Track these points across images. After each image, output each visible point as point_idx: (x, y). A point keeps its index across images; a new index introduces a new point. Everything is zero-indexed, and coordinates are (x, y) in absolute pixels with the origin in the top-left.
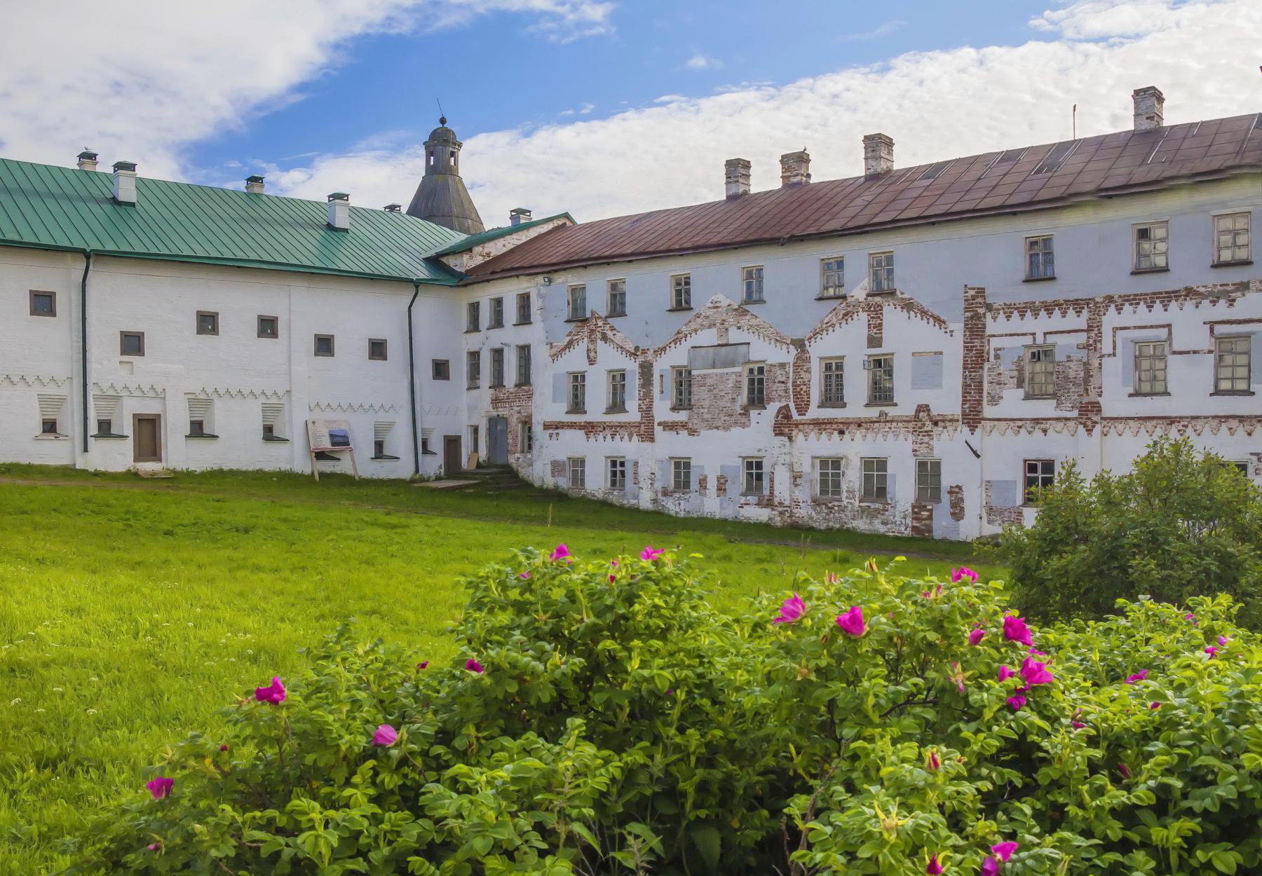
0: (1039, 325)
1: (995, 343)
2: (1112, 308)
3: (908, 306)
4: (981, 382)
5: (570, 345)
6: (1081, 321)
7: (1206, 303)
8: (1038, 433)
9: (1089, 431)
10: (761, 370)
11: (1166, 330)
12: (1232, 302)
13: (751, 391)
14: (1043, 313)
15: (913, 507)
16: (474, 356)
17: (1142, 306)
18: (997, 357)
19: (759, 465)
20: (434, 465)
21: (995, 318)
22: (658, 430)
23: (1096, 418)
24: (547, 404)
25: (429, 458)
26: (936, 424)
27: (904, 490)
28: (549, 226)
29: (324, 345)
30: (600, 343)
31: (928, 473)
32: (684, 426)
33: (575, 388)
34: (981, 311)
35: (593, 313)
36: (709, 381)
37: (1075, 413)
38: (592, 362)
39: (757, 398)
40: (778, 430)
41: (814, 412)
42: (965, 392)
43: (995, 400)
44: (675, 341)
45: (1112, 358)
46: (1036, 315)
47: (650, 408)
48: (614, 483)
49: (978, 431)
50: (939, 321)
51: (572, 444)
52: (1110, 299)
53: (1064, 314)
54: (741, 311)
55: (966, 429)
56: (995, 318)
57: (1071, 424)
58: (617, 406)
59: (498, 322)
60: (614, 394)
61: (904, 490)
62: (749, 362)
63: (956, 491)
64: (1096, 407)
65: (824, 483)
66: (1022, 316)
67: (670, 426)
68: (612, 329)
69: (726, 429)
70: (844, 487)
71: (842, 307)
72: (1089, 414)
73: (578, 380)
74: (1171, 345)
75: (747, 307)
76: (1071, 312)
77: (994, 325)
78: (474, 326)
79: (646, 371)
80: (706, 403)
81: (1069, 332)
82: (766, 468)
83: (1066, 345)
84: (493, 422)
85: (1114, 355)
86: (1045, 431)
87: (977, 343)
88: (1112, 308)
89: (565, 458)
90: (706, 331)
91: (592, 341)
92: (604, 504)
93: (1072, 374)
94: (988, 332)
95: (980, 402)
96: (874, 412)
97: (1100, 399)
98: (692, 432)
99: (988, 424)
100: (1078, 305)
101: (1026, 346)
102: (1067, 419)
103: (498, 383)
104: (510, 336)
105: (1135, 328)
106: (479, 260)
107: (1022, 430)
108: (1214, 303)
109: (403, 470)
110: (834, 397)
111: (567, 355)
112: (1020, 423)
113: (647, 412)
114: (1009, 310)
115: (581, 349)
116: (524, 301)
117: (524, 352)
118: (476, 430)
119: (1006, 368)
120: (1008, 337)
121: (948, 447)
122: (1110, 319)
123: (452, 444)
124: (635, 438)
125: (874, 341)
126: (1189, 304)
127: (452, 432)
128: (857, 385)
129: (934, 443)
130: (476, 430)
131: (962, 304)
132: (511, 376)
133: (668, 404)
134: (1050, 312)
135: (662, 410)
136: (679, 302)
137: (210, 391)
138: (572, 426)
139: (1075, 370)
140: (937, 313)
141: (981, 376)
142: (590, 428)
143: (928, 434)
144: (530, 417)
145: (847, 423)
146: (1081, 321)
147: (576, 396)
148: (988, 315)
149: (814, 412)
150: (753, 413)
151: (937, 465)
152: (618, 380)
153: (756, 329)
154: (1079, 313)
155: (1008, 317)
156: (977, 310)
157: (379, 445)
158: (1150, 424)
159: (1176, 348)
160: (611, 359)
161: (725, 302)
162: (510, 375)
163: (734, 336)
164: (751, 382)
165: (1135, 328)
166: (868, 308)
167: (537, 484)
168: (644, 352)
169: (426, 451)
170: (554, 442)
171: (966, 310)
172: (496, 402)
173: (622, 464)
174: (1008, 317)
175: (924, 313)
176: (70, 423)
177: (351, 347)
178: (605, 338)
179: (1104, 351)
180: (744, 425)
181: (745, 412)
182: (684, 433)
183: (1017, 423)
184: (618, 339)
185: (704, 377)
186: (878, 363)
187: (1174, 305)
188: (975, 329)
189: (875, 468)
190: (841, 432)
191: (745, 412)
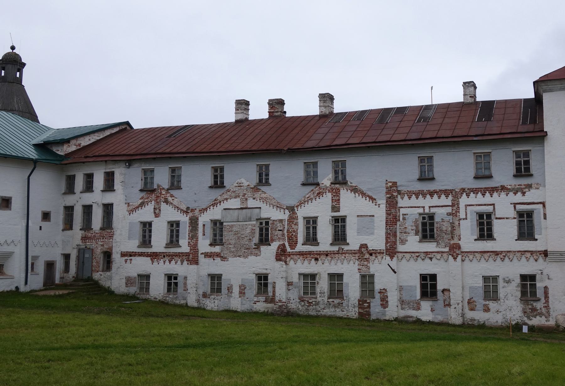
0: (427, 203)
1: (402, 211)
2: (464, 195)
3: (355, 190)
4: (396, 232)
5: (142, 205)
6: (449, 201)
7: (511, 194)
9: (455, 259)
11: (492, 206)
12: (524, 194)
13: (261, 235)
14: (428, 196)
15: (359, 301)
16: (69, 210)
17: (480, 195)
18: (404, 219)
19: (266, 277)
20: (37, 281)
21: (402, 198)
22: (201, 258)
26: (371, 255)
28: (116, 130)
30: (163, 206)
31: (367, 281)
32: (218, 255)
34: (395, 194)
35: (159, 186)
37: (447, 249)
38: (157, 215)
39: (264, 240)
41: (300, 247)
42: (387, 238)
43: (403, 242)
44: (213, 205)
45: (465, 221)
46: (424, 197)
47: (196, 245)
48: (169, 290)
49: (395, 259)
50: (372, 199)
51: (141, 265)
52: (463, 190)
53: (439, 197)
54: (256, 189)
55: (388, 258)
56: (402, 198)
57: (445, 255)
58: (173, 240)
60: (172, 236)
62: (260, 219)
63: (383, 292)
64: (459, 247)
65: (305, 287)
66: (417, 198)
67: (208, 255)
68: (172, 196)
69: (246, 257)
70: (318, 290)
71: (317, 190)
72: (455, 250)
73: (147, 227)
74: (495, 215)
75: (259, 187)
77: (403, 202)
78: (70, 190)
79: (194, 222)
80: (233, 242)
81: (442, 206)
82: (270, 280)
83: (441, 214)
84: (81, 252)
85: (466, 219)
86: (431, 259)
87: (393, 211)
88: (464, 195)
89: (136, 275)
90: (233, 200)
91: (158, 203)
92: (163, 303)
93: (444, 229)
94: (399, 205)
95: (395, 243)
96: (336, 248)
97: (460, 242)
98: (224, 259)
99: (400, 255)
100: (447, 193)
101: (420, 214)
102: (442, 252)
105: (476, 205)
107: (419, 258)
108: (515, 194)
110: (312, 239)
111: (140, 211)
112: (417, 254)
113: (194, 247)
115: (150, 207)
117: (108, 209)
118: (67, 257)
119: (409, 224)
121: (380, 269)
122: (464, 200)
123: (50, 266)
124: (185, 262)
125: (335, 208)
126: (503, 194)
127: (49, 259)
128: (325, 233)
129: (370, 265)
130: (67, 257)
133: (208, 242)
135: (204, 245)
136: (216, 183)
138: (141, 254)
139: (446, 226)
140: (370, 194)
141: (396, 228)
142: (154, 256)
144: (111, 249)
145: (320, 254)
146: (449, 201)
148: (399, 197)
149: (300, 247)
150: (263, 248)
151: (372, 276)
152: (174, 226)
153: (265, 200)
154: (447, 197)
155: (410, 198)
156: (393, 194)
158: (486, 255)
160: (169, 213)
161: (246, 183)
163: (251, 203)
164: (261, 230)
165: (476, 205)
166: (331, 190)
167: (117, 291)
168: (193, 210)
171: (387, 193)
172: (84, 239)
173: (176, 278)
174: (410, 198)
175: (363, 194)
178: (166, 202)
179: (461, 217)
180: (256, 255)
181: (257, 246)
182: (219, 259)
183: (416, 255)
184: (175, 202)
185: (232, 226)
187: (495, 194)
188: (392, 204)
189: (336, 278)
190: (316, 259)
191: (257, 246)
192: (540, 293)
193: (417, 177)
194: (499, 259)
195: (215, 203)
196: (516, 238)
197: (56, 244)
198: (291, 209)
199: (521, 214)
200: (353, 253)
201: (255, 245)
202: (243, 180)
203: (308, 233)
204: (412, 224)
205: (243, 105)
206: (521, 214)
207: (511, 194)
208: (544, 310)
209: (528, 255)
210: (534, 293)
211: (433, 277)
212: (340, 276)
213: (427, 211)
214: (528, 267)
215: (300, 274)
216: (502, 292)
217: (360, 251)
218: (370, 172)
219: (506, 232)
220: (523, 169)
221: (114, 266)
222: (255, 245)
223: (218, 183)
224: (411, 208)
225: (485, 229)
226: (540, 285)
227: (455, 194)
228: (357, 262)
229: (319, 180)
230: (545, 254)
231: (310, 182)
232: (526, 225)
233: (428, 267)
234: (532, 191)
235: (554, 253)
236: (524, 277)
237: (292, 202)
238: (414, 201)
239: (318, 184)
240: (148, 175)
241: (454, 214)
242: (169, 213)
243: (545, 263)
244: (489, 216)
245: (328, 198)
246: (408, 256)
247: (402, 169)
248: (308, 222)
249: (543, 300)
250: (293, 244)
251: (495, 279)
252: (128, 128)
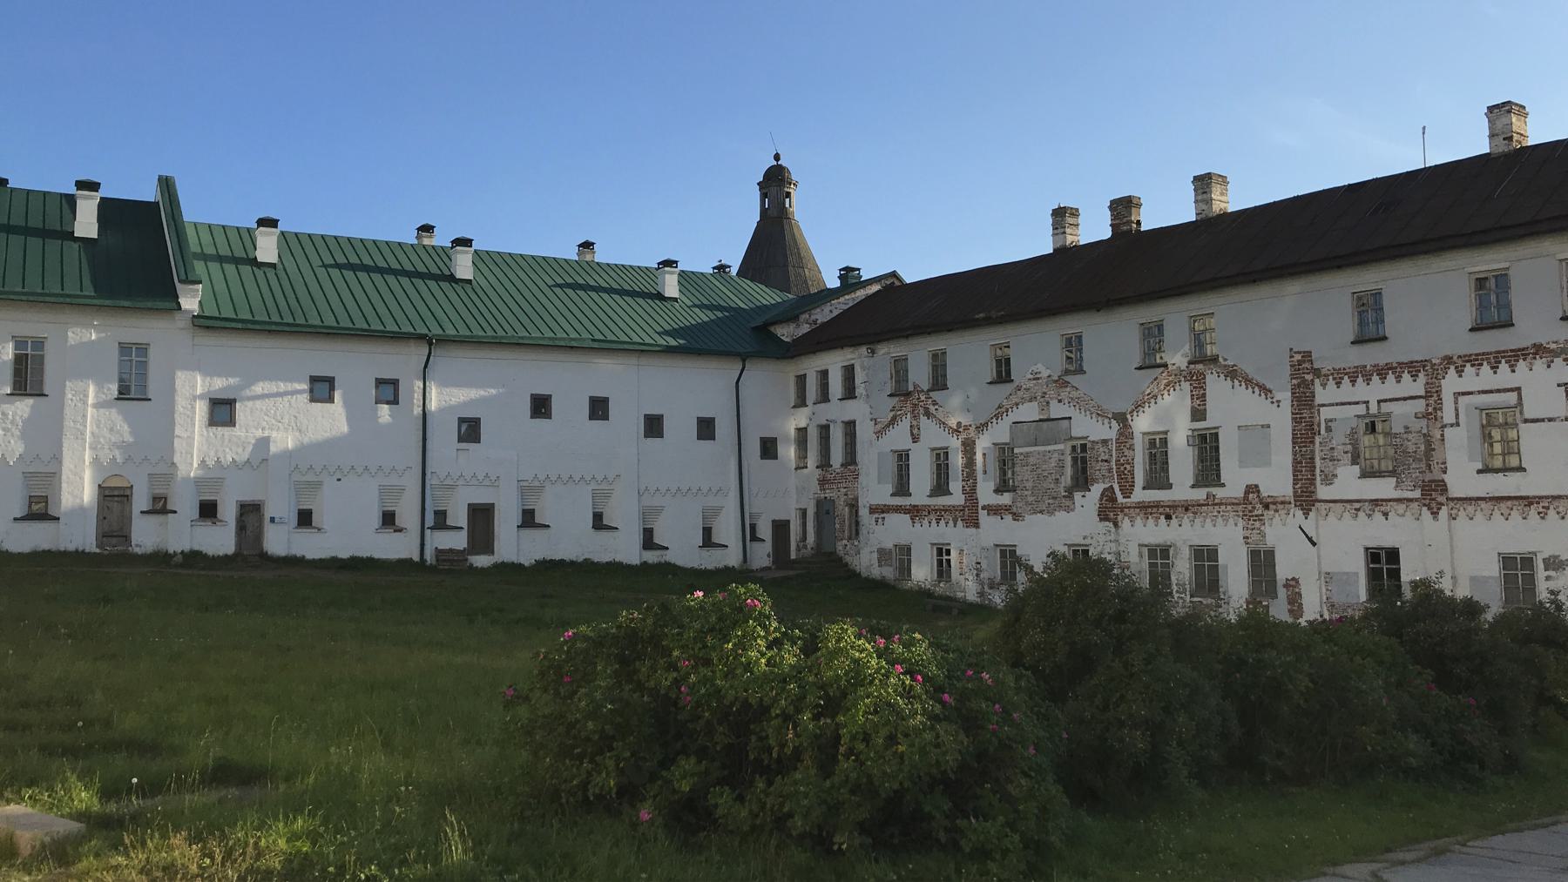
0: (1373, 391)
1: (1325, 413)
2: (1452, 370)
3: (1232, 374)
4: (1312, 459)
5: (893, 421)
6: (1418, 388)
8: (1378, 516)
9: (1435, 514)
10: (1084, 447)
14: (1375, 378)
15: (1248, 603)
17: (1486, 368)
18: (1328, 429)
20: (762, 556)
21: (1324, 385)
22: (983, 514)
23: (1442, 499)
24: (874, 488)
25: (756, 545)
26: (1267, 507)
27: (1237, 583)
29: (654, 426)
30: (923, 419)
31: (1262, 562)
33: (900, 468)
34: (1309, 377)
35: (915, 386)
36: (1032, 460)
37: (1417, 494)
38: (915, 439)
39: (1082, 480)
40: (1103, 515)
42: (1295, 471)
43: (1329, 479)
45: (1455, 429)
46: (1368, 381)
49: (1312, 514)
50: (1265, 391)
51: (896, 530)
52: (1448, 360)
53: (1398, 379)
54: (1061, 383)
55: (1299, 513)
56: (1324, 385)
58: (941, 488)
59: (824, 397)
60: (939, 475)
61: (1237, 583)
62: (1071, 438)
63: (1292, 584)
64: (1442, 487)
66: (1353, 382)
67: (994, 510)
69: (1051, 513)
70: (1173, 578)
72: (1434, 494)
73: (903, 458)
74: (1521, 413)
75: (1067, 378)
76: (1406, 376)
77: (1324, 394)
79: (969, 447)
80: (1029, 485)
81: (1405, 399)
83: (1403, 413)
84: (819, 504)
85: (1458, 424)
88: (1452, 370)
93: (1411, 448)
94: (1318, 400)
95: (1312, 481)
96: (1200, 494)
97: (1445, 477)
98: (1017, 517)
99: (1322, 506)
100: (1414, 368)
102: (1410, 500)
104: (837, 411)
105: (1480, 392)
106: (805, 329)
107: (1361, 514)
109: (732, 558)
110: (1159, 476)
111: (893, 432)
112: (1357, 505)
113: (971, 493)
114: (1338, 376)
115: (904, 425)
116: (849, 372)
117: (850, 426)
118: (804, 512)
119: (1339, 439)
120: (1339, 405)
121: (1282, 533)
122: (1451, 383)
123: (780, 528)
124: (960, 523)
125: (1198, 414)
126: (1539, 364)
129: (1267, 529)
130: (804, 512)
131: (1288, 371)
132: (837, 457)
133: (992, 486)
134: (1383, 378)
135: (986, 493)
136: (999, 373)
137: (542, 477)
138: (898, 509)
139: (1414, 444)
140: (1262, 381)
141: (1313, 452)
142: (915, 512)
143: (1260, 518)
144: (856, 499)
145: (1174, 506)
147: (900, 476)
148: (1317, 381)
149: (1140, 495)
150: (1077, 496)
151: (1270, 554)
153: (1076, 402)
154: (1415, 376)
155: (1338, 384)
156: (1305, 376)
157: (707, 532)
159: (1527, 416)
161: (1045, 373)
162: (834, 453)
163: (1057, 410)
164: (1075, 460)
165: (1480, 392)
167: (864, 575)
168: (966, 428)
169: (754, 538)
170: (879, 528)
171: (1293, 377)
172: (823, 482)
174: (1338, 384)
175: (1248, 381)
176: (408, 516)
177: (680, 427)
178: (928, 414)
179: (1446, 421)
180: (1069, 509)
181: (1070, 492)
183: (1355, 505)
184: (940, 415)
185: (1027, 455)
186: (1203, 438)
187: (1522, 365)
188: (1303, 400)
189: (1206, 557)
190: (1168, 517)
191: (1070, 492)
197: (787, 491)
202: (1040, 367)
211: (1393, 555)
213: (1374, 409)
221: (863, 531)
227: (1431, 370)
228: (1241, 523)
233: (1383, 532)
237: (1123, 406)
238: (1347, 391)
239: (1165, 366)
241: (1432, 414)
250: (1127, 491)
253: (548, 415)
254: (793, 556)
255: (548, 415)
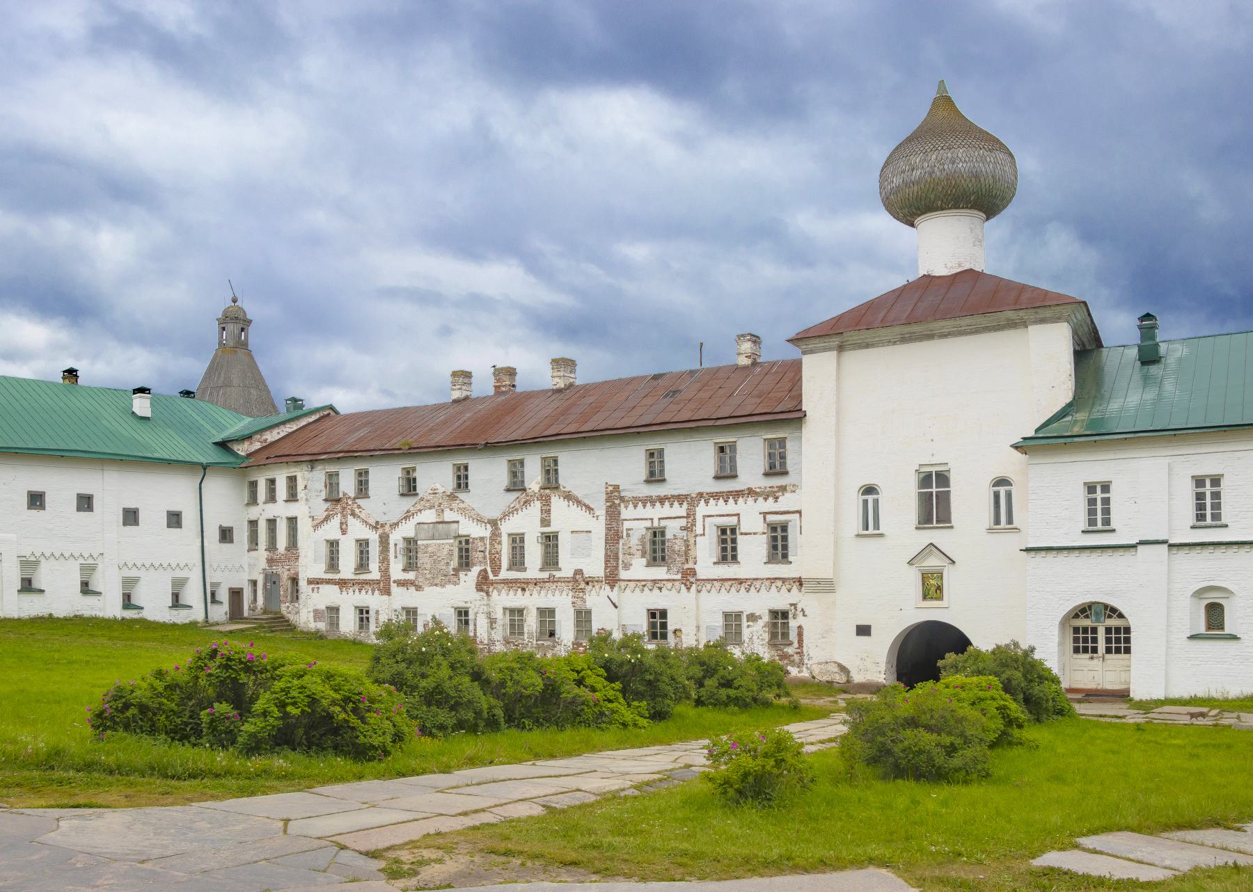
0: (656, 513)
1: (627, 525)
2: (702, 502)
3: (569, 497)
5: (327, 519)
6: (682, 511)
7: (761, 499)
8: (656, 591)
9: (688, 589)
10: (467, 542)
11: (735, 518)
12: (776, 498)
13: (461, 557)
14: (658, 504)
16: (253, 524)
17: (721, 501)
18: (628, 535)
19: (466, 613)
20: (220, 612)
21: (626, 507)
22: (394, 587)
23: (692, 580)
24: (311, 564)
25: (216, 607)
26: (587, 583)
27: (566, 632)
28: (313, 418)
29: (131, 517)
30: (350, 519)
31: (583, 617)
32: (412, 583)
33: (332, 552)
34: (617, 502)
35: (344, 494)
36: (430, 549)
37: (679, 576)
38: (344, 532)
39: (465, 562)
40: (479, 587)
41: (504, 574)
42: (607, 561)
43: (627, 566)
44: (405, 518)
47: (387, 569)
48: (361, 627)
49: (616, 589)
50: (589, 509)
51: (329, 595)
52: (701, 495)
53: (671, 505)
54: (452, 497)
55: (608, 588)
56: (626, 507)
57: (677, 584)
58: (362, 565)
59: (272, 498)
60: (361, 559)
62: (459, 536)
65: (512, 626)
66: (644, 506)
67: (402, 583)
68: (359, 507)
69: (443, 586)
70: (526, 630)
71: (523, 497)
72: (688, 577)
73: (333, 545)
76: (676, 504)
77: (627, 512)
78: (253, 501)
79: (384, 540)
80: (428, 566)
82: (471, 617)
83: (673, 529)
86: (660, 589)
87: (614, 524)
88: (702, 502)
89: (323, 607)
90: (428, 512)
91: (344, 516)
92: (355, 642)
93: (677, 548)
94: (623, 517)
95: (617, 567)
96: (545, 575)
98: (418, 588)
99: (623, 584)
100: (680, 499)
101: (648, 529)
103: (272, 545)
104: (281, 510)
106: (257, 446)
108: (766, 499)
109: (197, 614)
110: (518, 562)
111: (326, 527)
113: (385, 572)
114: (636, 501)
115: (336, 521)
116: (292, 480)
117: (292, 521)
118: (254, 583)
119: (634, 541)
120: (637, 522)
121: (596, 600)
123: (236, 594)
124: (377, 592)
125: (545, 522)
126: (750, 500)
127: (236, 585)
128: (534, 554)
129: (587, 597)
131: (604, 496)
132: (282, 542)
133: (401, 566)
134: (662, 503)
135: (396, 571)
137: (38, 554)
138: (329, 582)
139: (679, 546)
140: (587, 502)
142: (343, 584)
143: (583, 590)
144: (297, 574)
146: (682, 511)
147: (332, 559)
149: (504, 574)
150: (462, 575)
151: (589, 612)
152: (363, 545)
153: (463, 511)
155: (635, 507)
156: (615, 499)
157: (176, 597)
158: (727, 584)
159: (743, 530)
160: (358, 530)
161: (441, 490)
162: (280, 542)
163: (448, 516)
164: (460, 550)
166: (541, 498)
168: (382, 526)
169: (214, 601)
170: (315, 595)
171: (607, 501)
172: (270, 561)
173: (367, 612)
174: (635, 507)
175: (578, 502)
177: (152, 517)
178: (353, 514)
180: (455, 584)
182: (413, 588)
183: (642, 584)
184: (362, 516)
185: (427, 546)
186: (548, 538)
187: (741, 500)
188: (613, 514)
189: (547, 614)
190: (523, 590)
191: (456, 571)
192: (793, 636)
193: (644, 478)
194: (743, 589)
195: (407, 516)
196: (765, 560)
197: (241, 567)
198: (494, 523)
199: (773, 528)
200: (565, 581)
201: (454, 569)
202: (438, 486)
203: (514, 556)
204: (637, 542)
205: (463, 376)
206: (773, 528)
207: (761, 499)
208: (796, 658)
209: (779, 583)
210: (785, 635)
211: (664, 614)
212: (552, 612)
213: (656, 524)
214: (780, 600)
215: (505, 609)
216: (746, 633)
217: (575, 580)
218: (588, 470)
219: (753, 550)
220: (777, 467)
221: (302, 597)
222: (454, 569)
223: (410, 487)
224: (637, 522)
225: (728, 548)
226: (793, 624)
227: (690, 500)
228: (571, 594)
229: (526, 485)
230: (800, 582)
231: (516, 484)
232: (779, 543)
233: (657, 600)
234: (787, 495)
235: (810, 580)
236: (774, 614)
237: (496, 515)
238: (641, 511)
239: (525, 490)
240: (332, 482)
241: (688, 529)
242: (358, 530)
243: (800, 595)
244: (733, 531)
245: (537, 506)
246: (632, 584)
247: (623, 465)
248: (514, 541)
249: (796, 644)
250: (496, 571)
251: (738, 616)
252: (332, 413)
253: (42, 507)
254: (246, 614)
255: (42, 507)
